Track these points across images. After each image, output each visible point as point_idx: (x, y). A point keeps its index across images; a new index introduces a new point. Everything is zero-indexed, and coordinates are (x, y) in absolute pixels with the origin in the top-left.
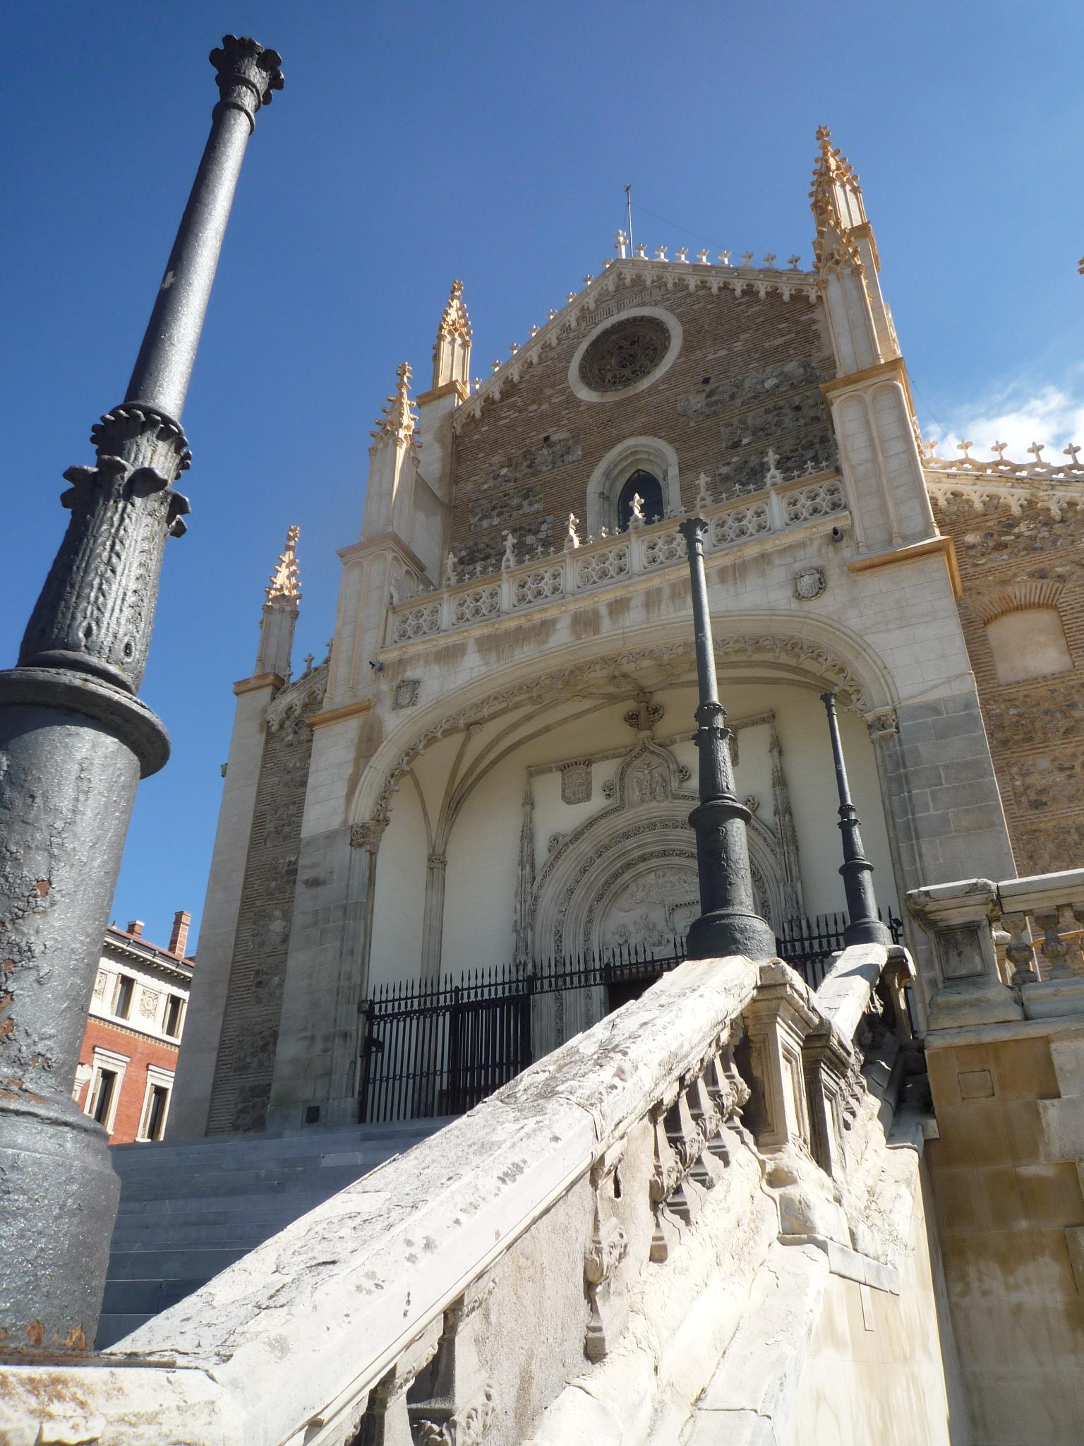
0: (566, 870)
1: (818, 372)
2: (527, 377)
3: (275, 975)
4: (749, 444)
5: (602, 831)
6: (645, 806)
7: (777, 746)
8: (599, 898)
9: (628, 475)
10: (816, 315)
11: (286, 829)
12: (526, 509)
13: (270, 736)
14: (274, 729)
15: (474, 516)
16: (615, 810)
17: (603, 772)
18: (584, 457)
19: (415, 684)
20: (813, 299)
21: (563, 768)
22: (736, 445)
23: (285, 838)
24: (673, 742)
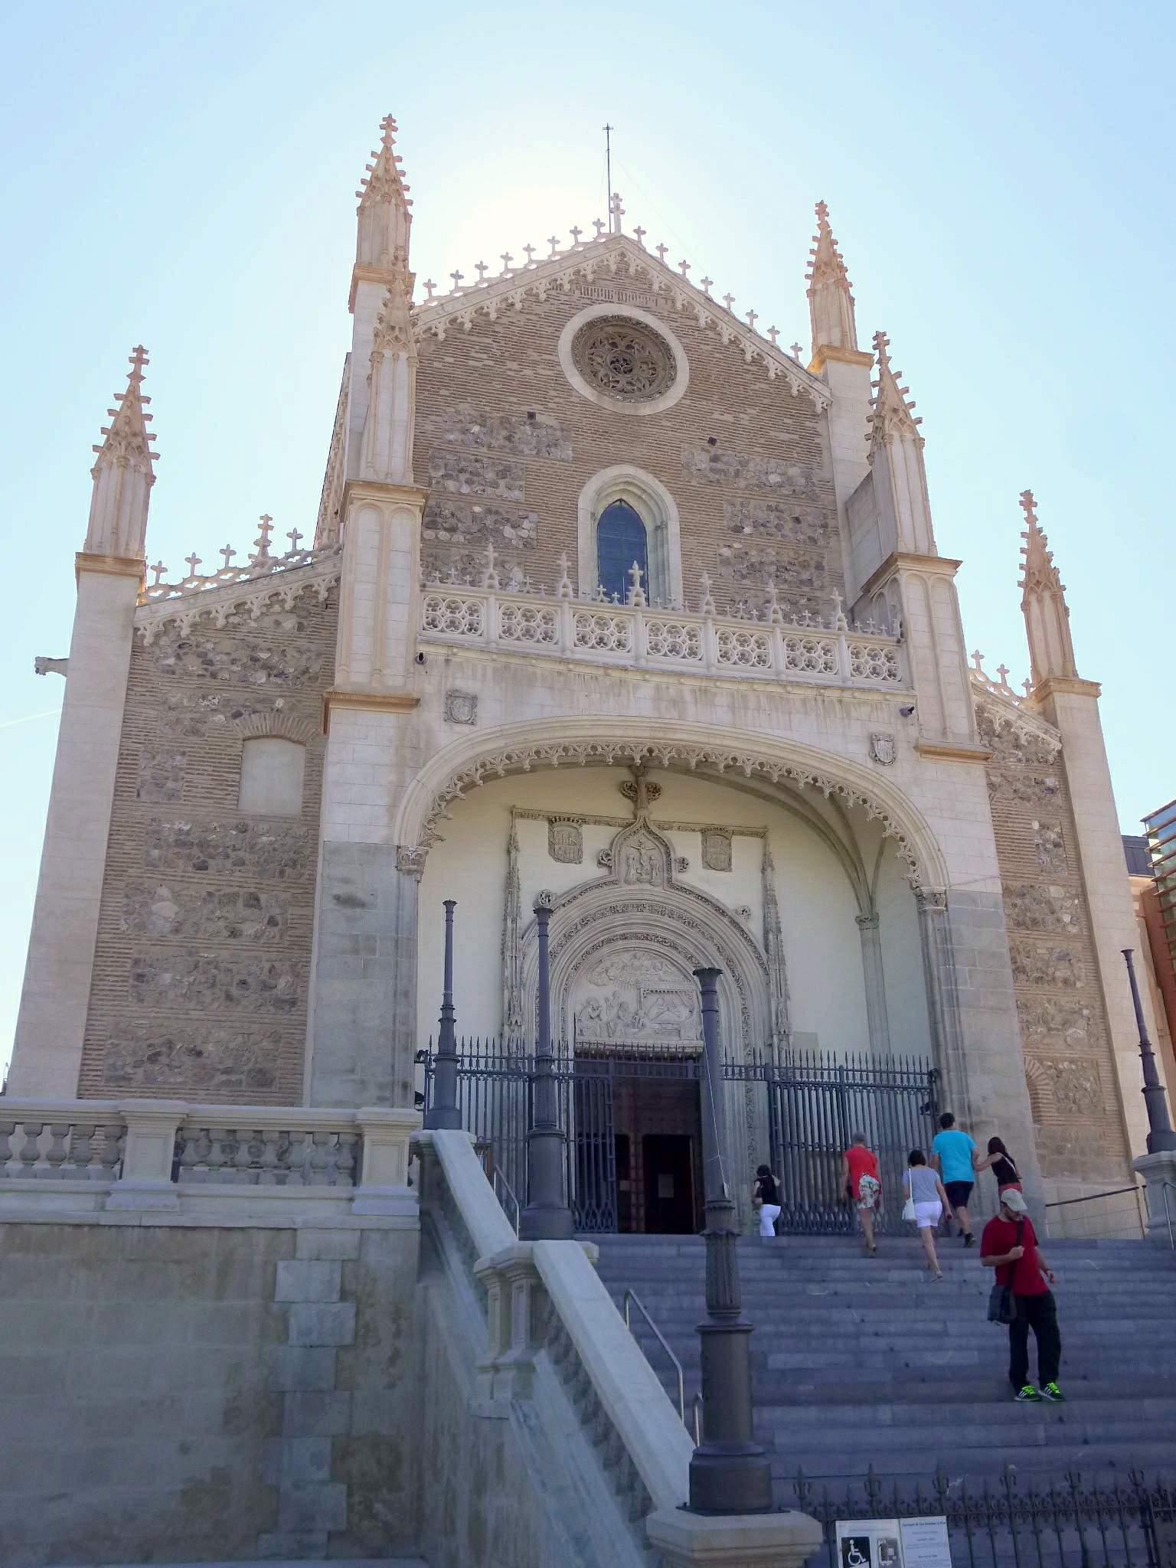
1: (817, 490)
2: (504, 320)
3: (166, 970)
4: (750, 535)
5: (594, 900)
6: (637, 886)
7: (766, 865)
8: (576, 968)
9: (611, 500)
10: (820, 427)
11: (170, 784)
12: (502, 490)
13: (137, 650)
14: (147, 642)
15: (436, 468)
16: (613, 883)
17: (595, 838)
18: (575, 460)
19: (473, 700)
20: (819, 410)
21: (551, 822)
22: (738, 529)
23: (172, 796)
24: (671, 828)
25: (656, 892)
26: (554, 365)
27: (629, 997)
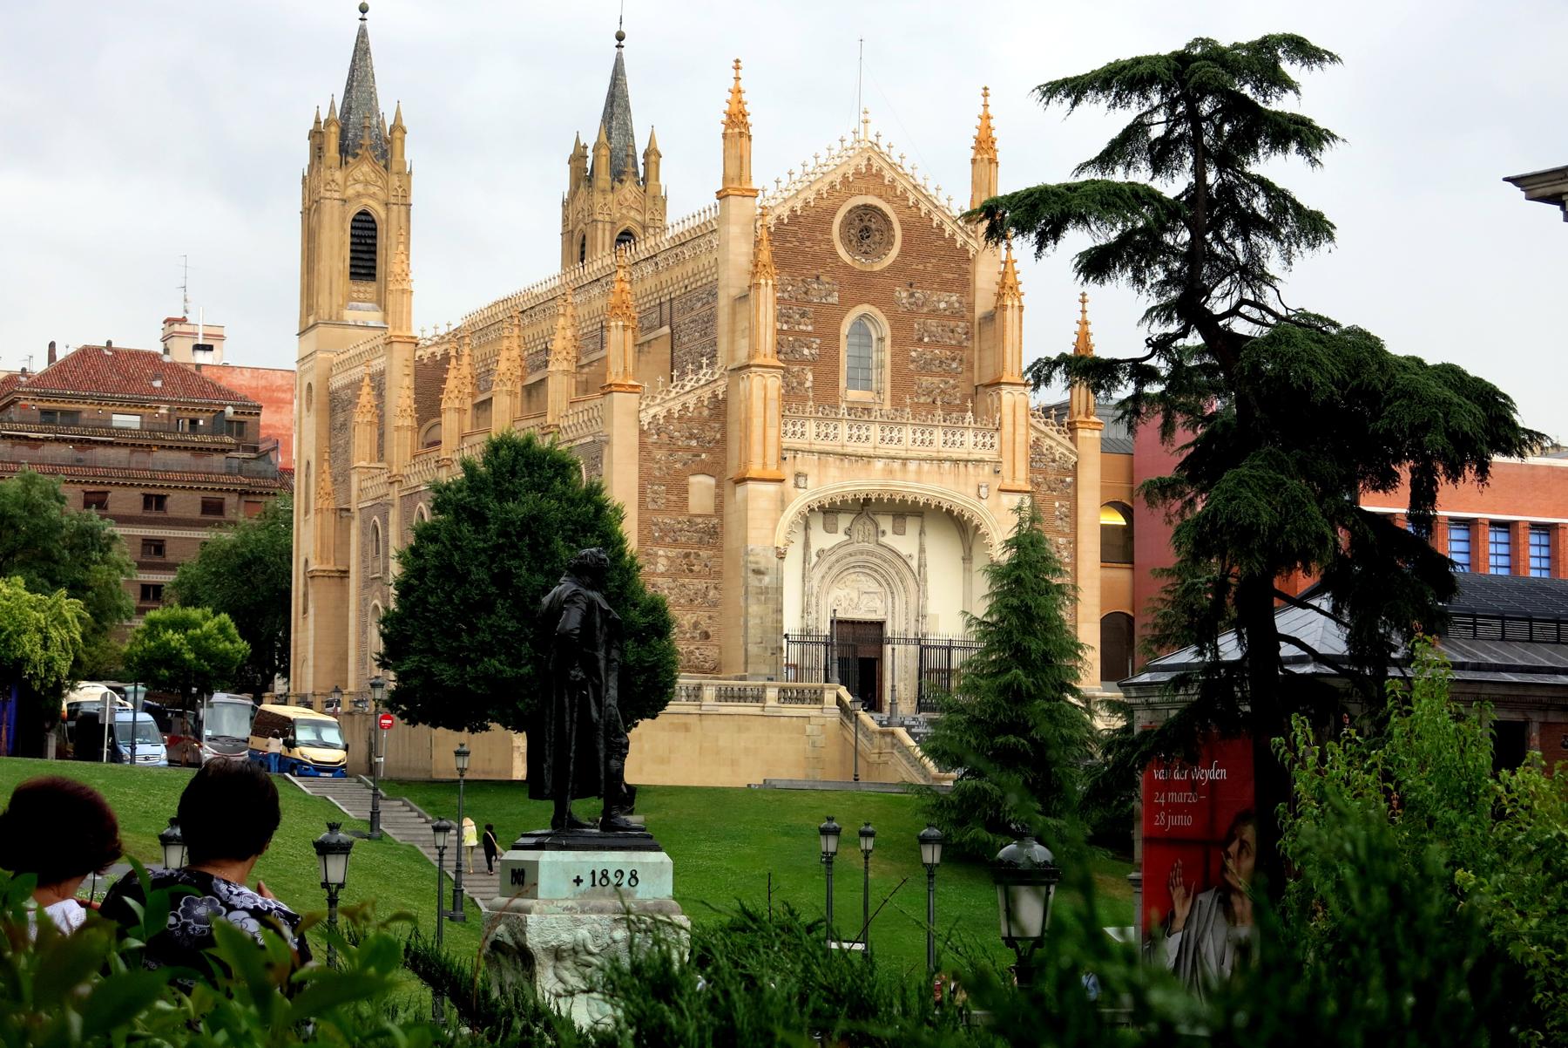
0: (824, 568)
5: (842, 552)
13: (642, 432)
17: (844, 521)
22: (921, 340)
25: (871, 547)
26: (830, 241)
27: (854, 595)
